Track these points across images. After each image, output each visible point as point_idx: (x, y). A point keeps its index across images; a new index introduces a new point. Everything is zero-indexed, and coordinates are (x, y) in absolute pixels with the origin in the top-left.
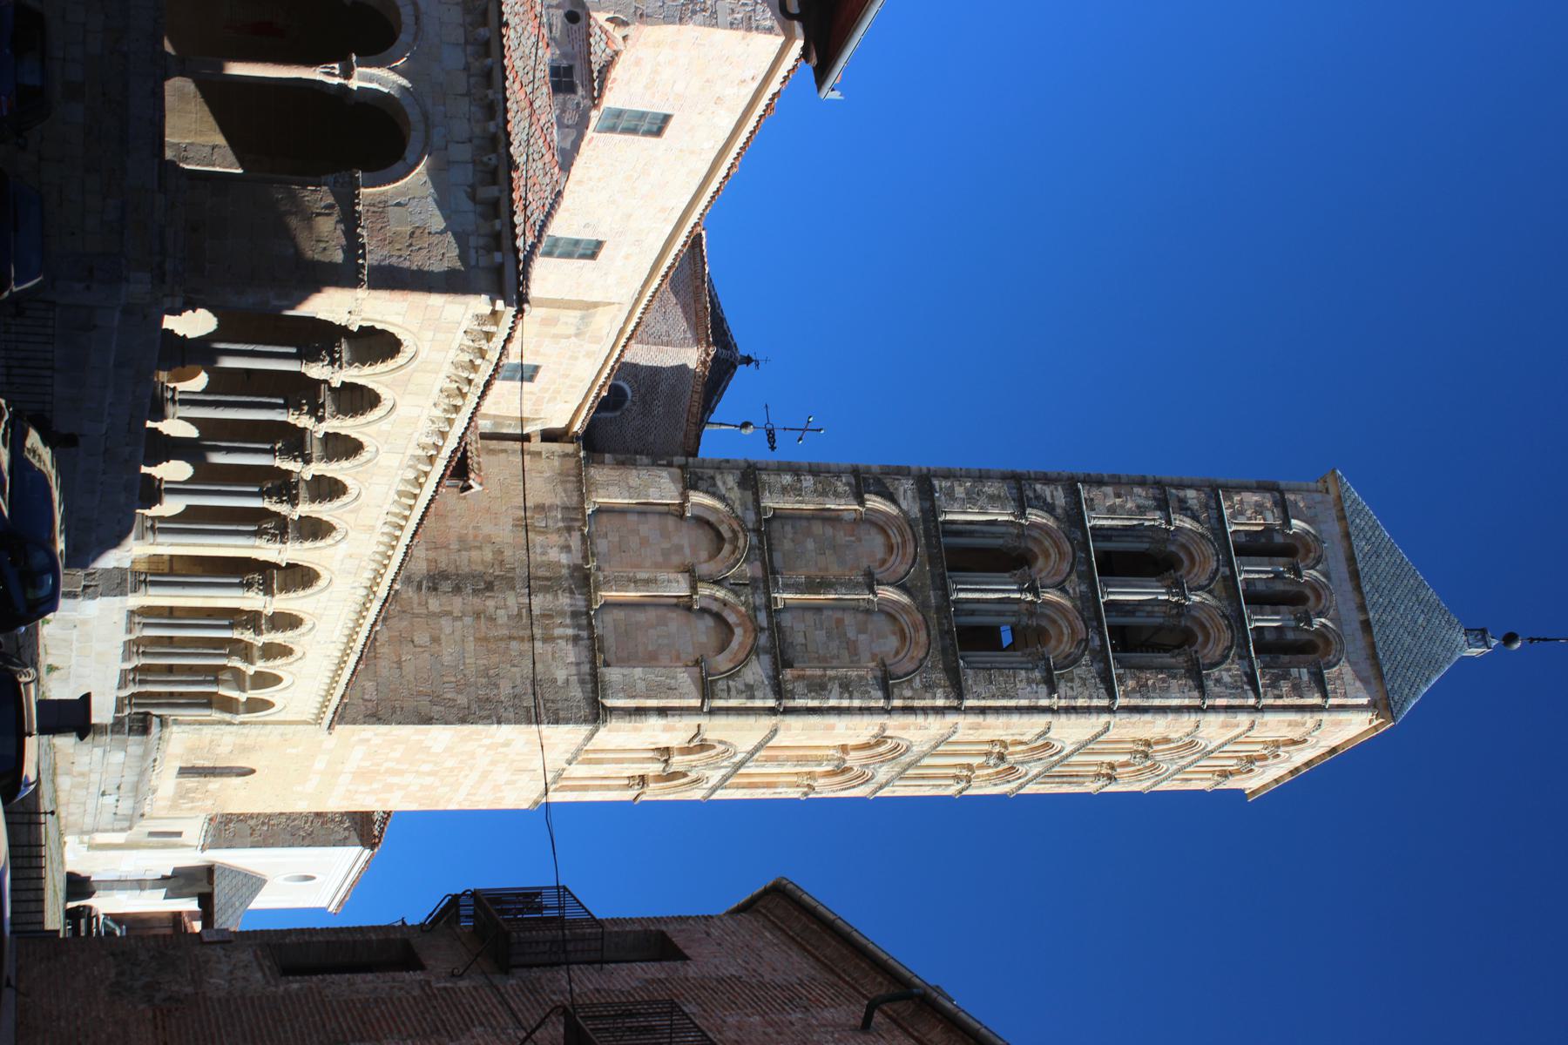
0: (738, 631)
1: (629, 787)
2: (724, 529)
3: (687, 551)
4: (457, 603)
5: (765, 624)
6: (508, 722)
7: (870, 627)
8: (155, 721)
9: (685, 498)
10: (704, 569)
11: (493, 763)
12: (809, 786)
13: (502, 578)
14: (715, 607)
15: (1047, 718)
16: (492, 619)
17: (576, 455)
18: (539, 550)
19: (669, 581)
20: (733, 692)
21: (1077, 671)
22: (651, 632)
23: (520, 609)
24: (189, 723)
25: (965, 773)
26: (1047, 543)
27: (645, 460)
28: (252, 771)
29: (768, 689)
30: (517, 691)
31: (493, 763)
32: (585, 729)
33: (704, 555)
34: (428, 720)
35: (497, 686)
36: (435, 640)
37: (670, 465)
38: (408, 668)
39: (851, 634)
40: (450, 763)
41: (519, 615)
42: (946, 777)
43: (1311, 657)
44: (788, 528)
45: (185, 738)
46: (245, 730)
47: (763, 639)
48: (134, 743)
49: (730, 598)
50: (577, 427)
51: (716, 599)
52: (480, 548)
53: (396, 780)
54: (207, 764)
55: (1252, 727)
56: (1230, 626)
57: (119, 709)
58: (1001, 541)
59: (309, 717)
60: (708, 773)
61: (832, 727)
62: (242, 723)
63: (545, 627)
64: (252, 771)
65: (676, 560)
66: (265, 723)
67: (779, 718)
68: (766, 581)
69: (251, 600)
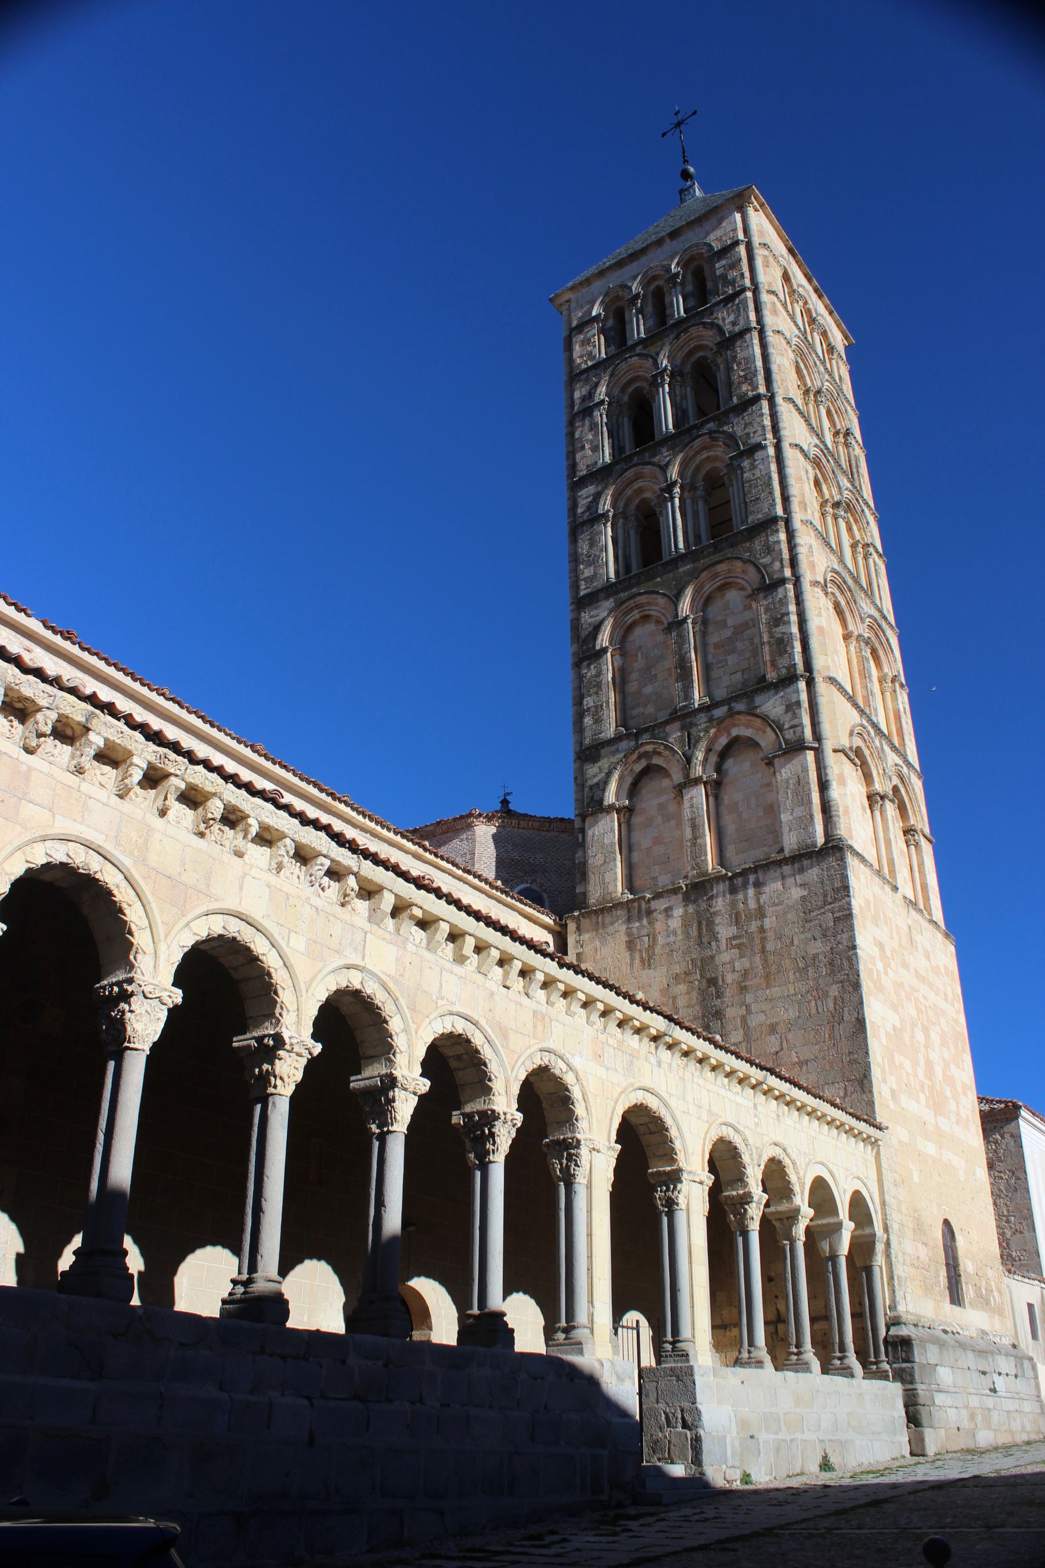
0: (735, 732)
1: (917, 845)
2: (638, 768)
3: (663, 799)
4: (733, 1013)
5: (725, 708)
6: (852, 938)
7: (719, 618)
8: (893, 1331)
9: (612, 807)
10: (677, 777)
11: (905, 965)
12: (893, 681)
13: (702, 970)
14: (713, 759)
15: (785, 445)
16: (746, 974)
17: (577, 920)
18: (672, 939)
19: (692, 806)
20: (796, 722)
22: (745, 816)
23: (733, 947)
24: (893, 1291)
25: (860, 549)
26: (629, 492)
27: (580, 854)
28: (946, 1223)
29: (788, 690)
30: (818, 935)
31: (905, 965)
32: (851, 861)
33: (666, 783)
34: (860, 1024)
35: (815, 957)
36: (773, 1029)
37: (583, 831)
38: (806, 1053)
39: (728, 633)
40: (913, 1012)
41: (738, 946)
42: (867, 566)
43: (706, 268)
44: (635, 712)
45: (911, 1294)
46: (894, 1227)
47: (740, 706)
48: (924, 1355)
49: (703, 746)
50: (548, 920)
51: (706, 759)
52: (674, 998)
53: (938, 1070)
54: (943, 1272)
55: (773, 293)
56: (685, 330)
57: (883, 1376)
58: (632, 533)
59: (870, 1152)
60: (890, 762)
61: (821, 629)
62: (886, 1229)
63: (749, 918)
64: (946, 1223)
65: (672, 808)
66: (883, 1204)
67: (816, 674)
68: (683, 717)
69: (692, 1201)
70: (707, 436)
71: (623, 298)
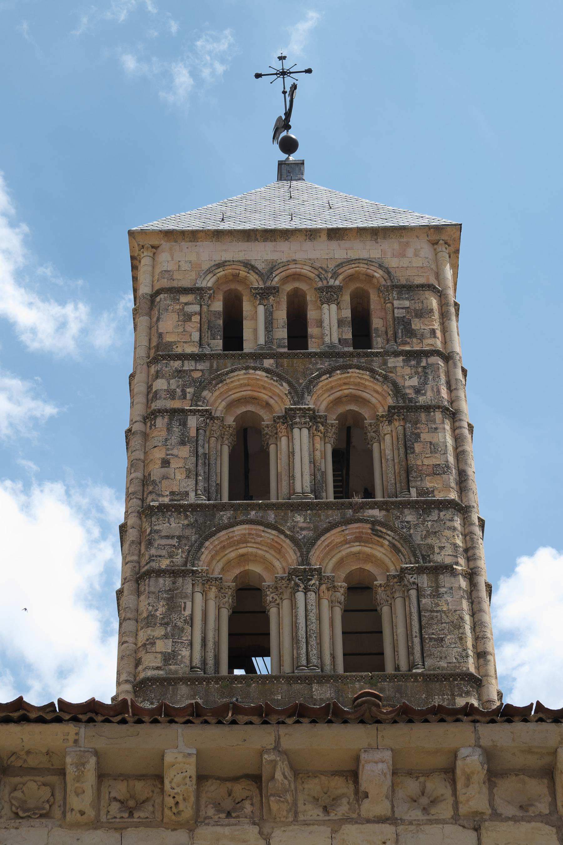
21: (418, 540)
56: (345, 368)
70: (369, 526)
71: (243, 281)
